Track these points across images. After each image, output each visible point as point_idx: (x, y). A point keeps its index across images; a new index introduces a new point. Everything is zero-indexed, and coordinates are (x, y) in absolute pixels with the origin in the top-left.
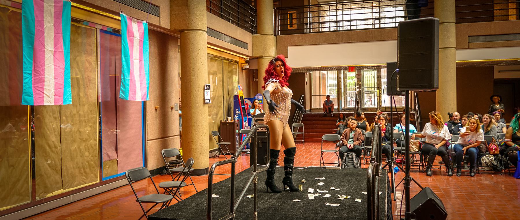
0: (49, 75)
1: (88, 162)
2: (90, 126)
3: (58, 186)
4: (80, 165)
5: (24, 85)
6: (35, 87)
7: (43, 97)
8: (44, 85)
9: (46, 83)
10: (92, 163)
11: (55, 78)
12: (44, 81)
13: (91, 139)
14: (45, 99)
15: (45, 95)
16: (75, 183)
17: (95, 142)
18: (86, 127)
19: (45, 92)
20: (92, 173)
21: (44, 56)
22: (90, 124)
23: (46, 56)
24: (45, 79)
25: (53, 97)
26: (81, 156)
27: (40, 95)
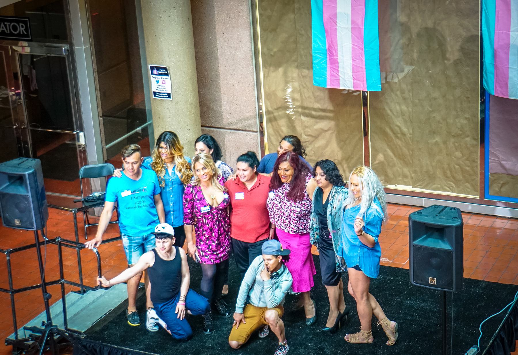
0: (343, 56)
1: (459, 165)
2: (466, 118)
3: (406, 180)
4: (446, 166)
5: (314, 65)
6: (330, 67)
7: (339, 80)
8: (338, 67)
9: (340, 65)
10: (468, 168)
11: (353, 60)
12: (338, 63)
13: (468, 136)
14: (341, 82)
15: (340, 78)
16: (434, 186)
17: (474, 142)
18: (457, 117)
19: (340, 74)
20: (467, 182)
21: (336, 35)
22: (467, 116)
23: (338, 34)
24: (339, 61)
25: (352, 80)
26: (447, 155)
27: (336, 77)
